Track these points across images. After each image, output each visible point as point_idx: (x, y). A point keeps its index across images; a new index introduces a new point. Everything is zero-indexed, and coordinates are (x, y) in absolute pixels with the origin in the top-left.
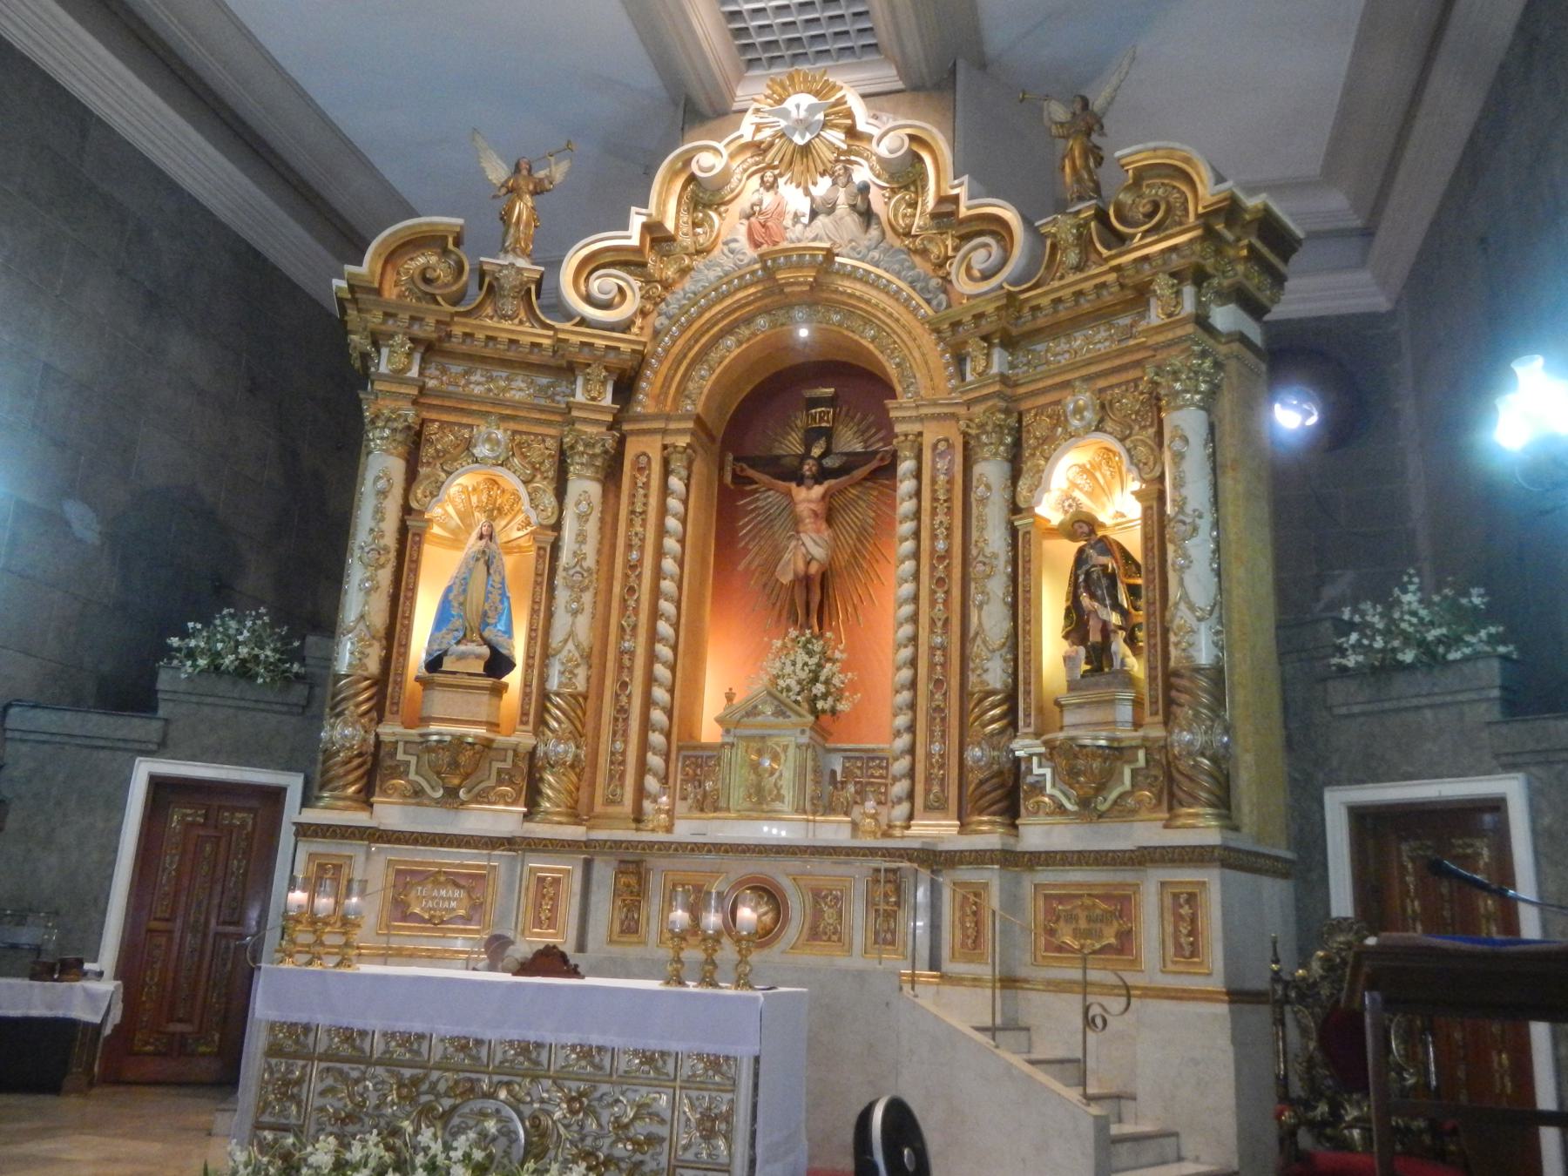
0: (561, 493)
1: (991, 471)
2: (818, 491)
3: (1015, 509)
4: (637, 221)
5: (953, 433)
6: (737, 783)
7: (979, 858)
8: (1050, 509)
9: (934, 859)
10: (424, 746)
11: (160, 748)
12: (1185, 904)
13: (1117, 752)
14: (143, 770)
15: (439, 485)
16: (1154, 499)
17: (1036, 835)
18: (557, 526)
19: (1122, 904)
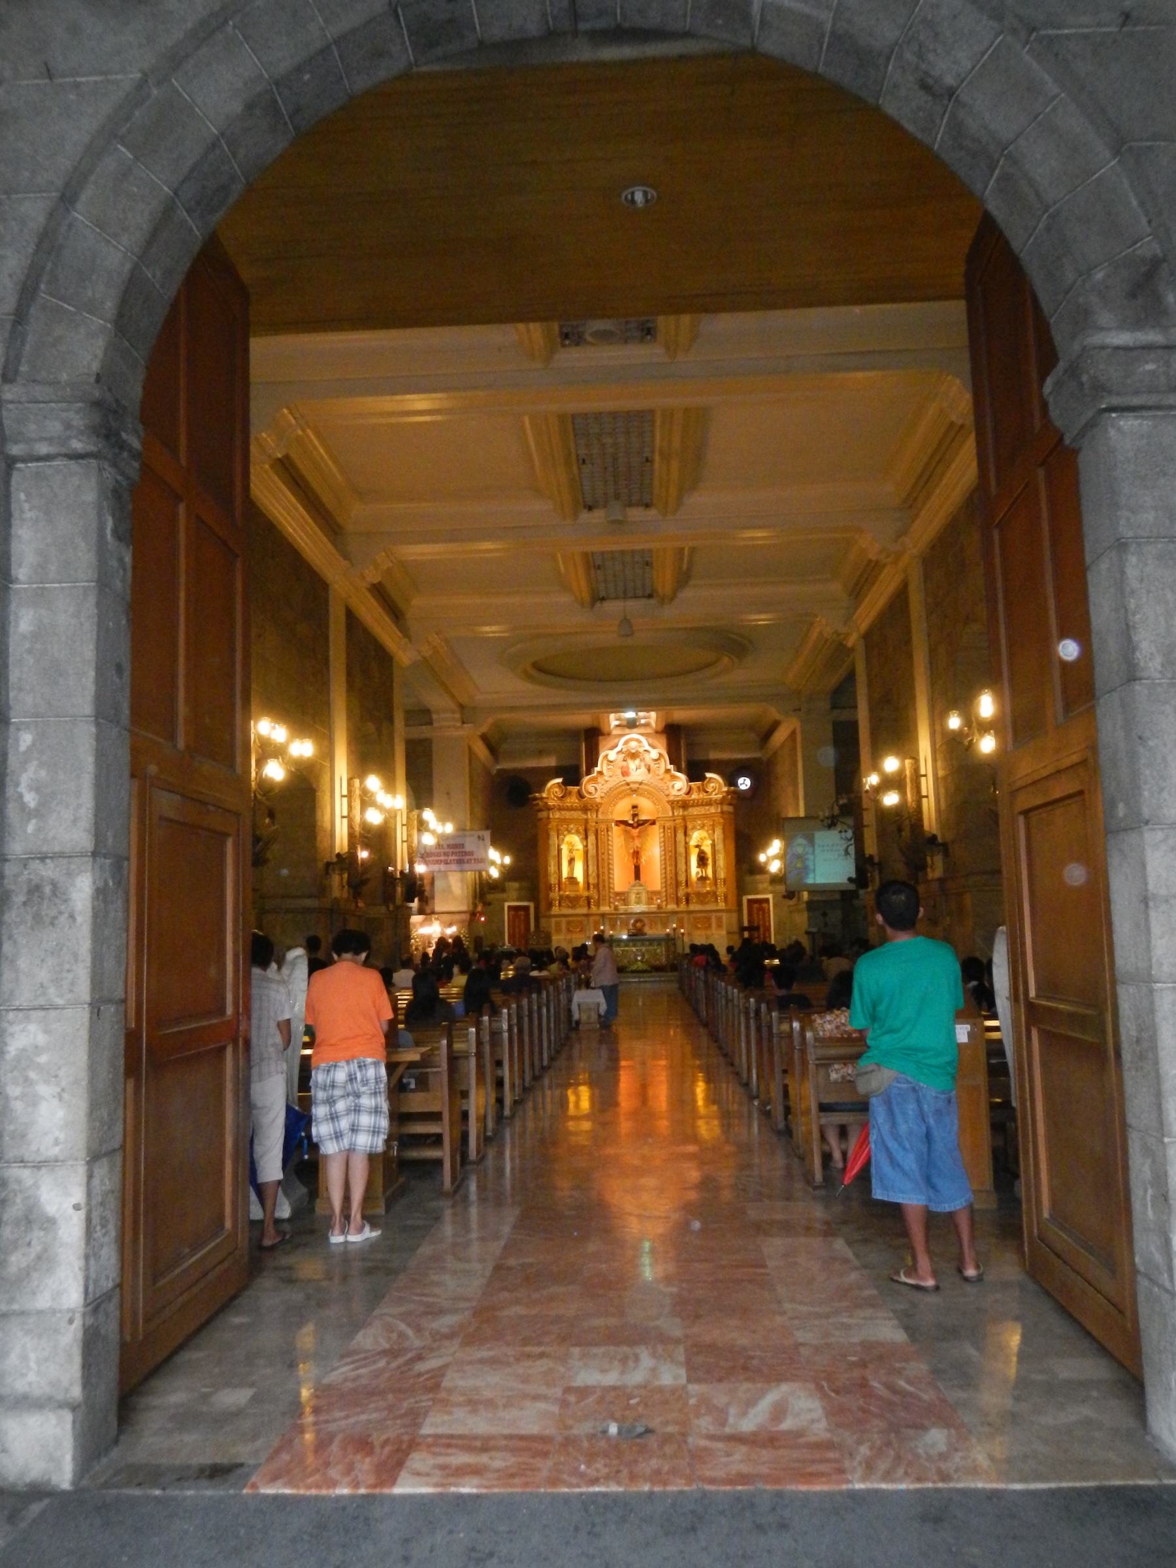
0: (586, 838)
1: (680, 836)
2: (637, 830)
3: (686, 843)
4: (597, 769)
5: (671, 824)
6: (633, 897)
7: (682, 912)
8: (693, 843)
9: (674, 913)
10: (568, 897)
11: (506, 901)
12: (719, 919)
13: (708, 893)
14: (506, 904)
15: (563, 840)
16: (713, 846)
17: (692, 907)
18: (587, 846)
19: (709, 919)
